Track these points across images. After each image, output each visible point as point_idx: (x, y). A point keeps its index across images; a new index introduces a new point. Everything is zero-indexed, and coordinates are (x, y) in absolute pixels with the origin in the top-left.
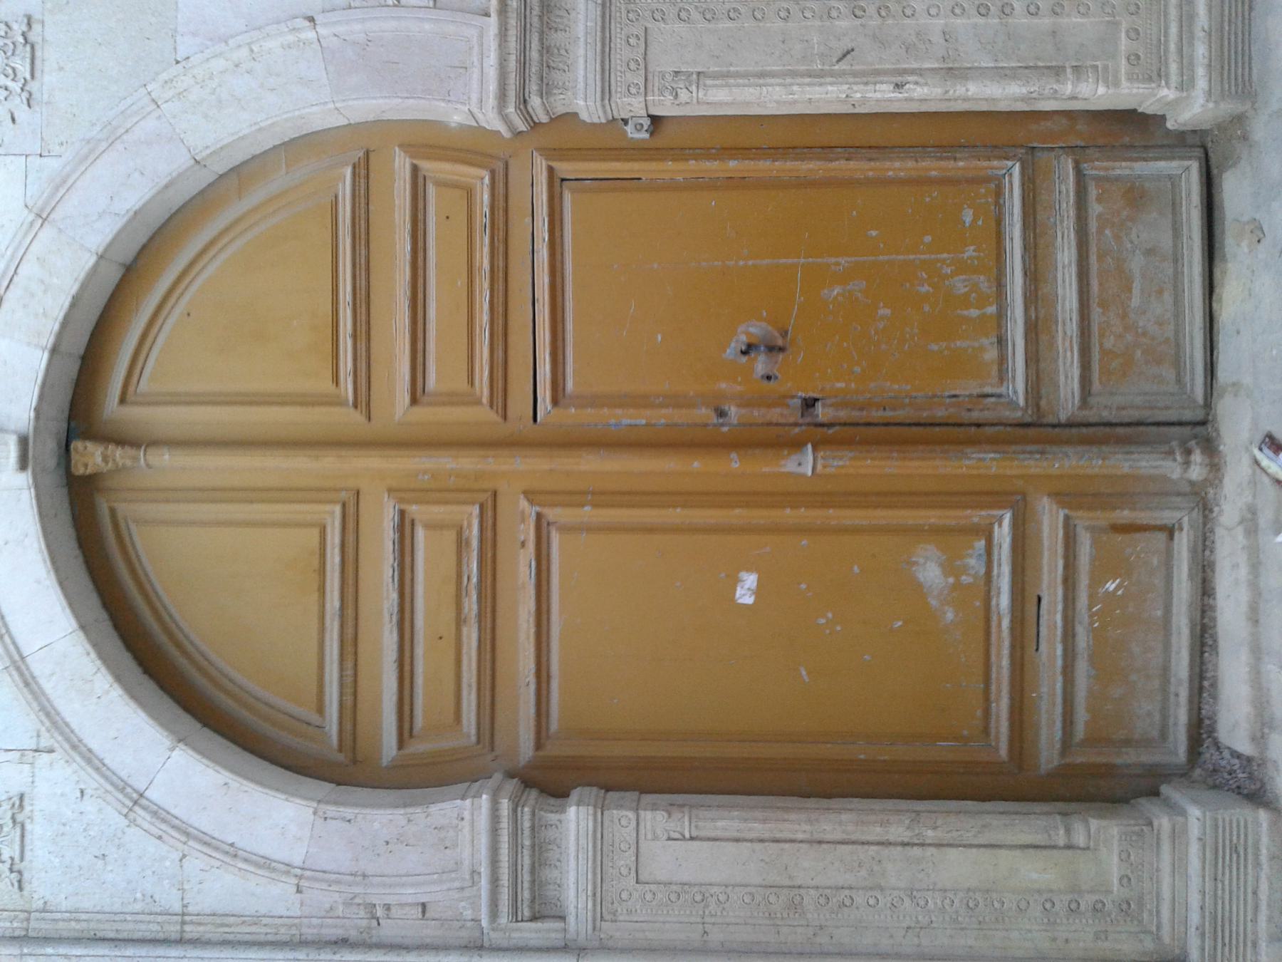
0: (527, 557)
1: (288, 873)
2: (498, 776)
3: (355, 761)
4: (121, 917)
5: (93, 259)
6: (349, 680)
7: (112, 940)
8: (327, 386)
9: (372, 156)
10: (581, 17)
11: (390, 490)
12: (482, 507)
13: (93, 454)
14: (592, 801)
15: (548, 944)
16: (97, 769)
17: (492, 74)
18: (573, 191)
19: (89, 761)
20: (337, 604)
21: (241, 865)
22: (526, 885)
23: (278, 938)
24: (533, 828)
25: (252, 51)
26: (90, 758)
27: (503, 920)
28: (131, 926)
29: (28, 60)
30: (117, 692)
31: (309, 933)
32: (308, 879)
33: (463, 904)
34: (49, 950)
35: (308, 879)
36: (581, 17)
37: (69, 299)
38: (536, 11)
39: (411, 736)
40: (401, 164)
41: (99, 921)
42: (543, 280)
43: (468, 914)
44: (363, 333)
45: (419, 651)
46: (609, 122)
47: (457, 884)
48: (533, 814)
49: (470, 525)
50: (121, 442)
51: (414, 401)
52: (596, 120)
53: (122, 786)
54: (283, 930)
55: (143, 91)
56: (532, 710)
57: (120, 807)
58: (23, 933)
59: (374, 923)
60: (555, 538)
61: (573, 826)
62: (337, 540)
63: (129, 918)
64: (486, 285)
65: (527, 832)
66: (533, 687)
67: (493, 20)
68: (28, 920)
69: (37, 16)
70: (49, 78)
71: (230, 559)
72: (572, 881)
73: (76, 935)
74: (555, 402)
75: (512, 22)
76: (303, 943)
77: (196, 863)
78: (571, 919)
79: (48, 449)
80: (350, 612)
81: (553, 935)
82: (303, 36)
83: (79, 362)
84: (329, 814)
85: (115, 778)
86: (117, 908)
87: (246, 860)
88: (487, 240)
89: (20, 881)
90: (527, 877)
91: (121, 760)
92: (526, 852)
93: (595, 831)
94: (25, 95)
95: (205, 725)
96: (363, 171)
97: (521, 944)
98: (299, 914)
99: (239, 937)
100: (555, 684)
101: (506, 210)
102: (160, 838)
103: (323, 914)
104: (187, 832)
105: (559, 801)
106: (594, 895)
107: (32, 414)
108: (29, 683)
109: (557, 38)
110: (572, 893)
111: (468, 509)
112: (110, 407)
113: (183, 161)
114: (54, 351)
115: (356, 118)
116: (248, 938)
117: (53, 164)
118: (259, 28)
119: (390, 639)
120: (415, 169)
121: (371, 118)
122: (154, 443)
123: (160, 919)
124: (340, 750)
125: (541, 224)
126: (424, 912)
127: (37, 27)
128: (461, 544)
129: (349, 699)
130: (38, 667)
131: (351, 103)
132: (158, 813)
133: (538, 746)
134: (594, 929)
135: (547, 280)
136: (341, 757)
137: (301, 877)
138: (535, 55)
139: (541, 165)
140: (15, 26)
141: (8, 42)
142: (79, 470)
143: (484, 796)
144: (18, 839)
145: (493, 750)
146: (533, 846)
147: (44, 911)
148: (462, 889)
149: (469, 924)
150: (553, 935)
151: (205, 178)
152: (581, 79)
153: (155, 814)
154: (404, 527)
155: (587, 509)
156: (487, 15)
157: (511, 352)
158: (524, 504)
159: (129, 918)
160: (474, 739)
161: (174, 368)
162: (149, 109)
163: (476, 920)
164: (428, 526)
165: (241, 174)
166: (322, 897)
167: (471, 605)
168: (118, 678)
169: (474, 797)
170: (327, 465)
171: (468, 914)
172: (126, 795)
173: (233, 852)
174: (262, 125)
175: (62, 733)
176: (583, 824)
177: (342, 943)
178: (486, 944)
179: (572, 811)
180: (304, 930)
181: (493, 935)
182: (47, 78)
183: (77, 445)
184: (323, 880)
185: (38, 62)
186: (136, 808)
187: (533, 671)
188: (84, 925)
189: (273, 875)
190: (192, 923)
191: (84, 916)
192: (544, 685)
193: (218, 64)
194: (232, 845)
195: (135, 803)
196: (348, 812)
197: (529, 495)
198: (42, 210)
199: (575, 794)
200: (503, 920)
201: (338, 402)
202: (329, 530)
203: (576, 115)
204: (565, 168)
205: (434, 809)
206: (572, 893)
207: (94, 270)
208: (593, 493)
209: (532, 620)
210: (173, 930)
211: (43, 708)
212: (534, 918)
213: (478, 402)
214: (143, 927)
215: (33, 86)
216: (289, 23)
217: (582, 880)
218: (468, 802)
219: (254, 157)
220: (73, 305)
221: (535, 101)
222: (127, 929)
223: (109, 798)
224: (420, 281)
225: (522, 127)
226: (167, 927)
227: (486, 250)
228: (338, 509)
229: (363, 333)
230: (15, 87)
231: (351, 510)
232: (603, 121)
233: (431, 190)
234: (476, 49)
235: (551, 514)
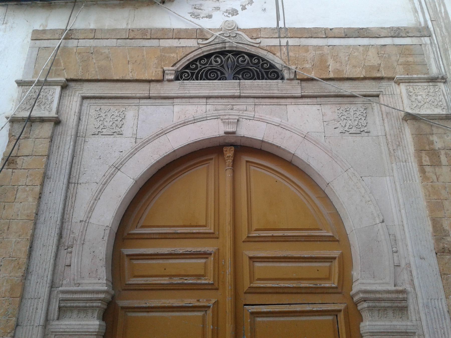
0: (192, 302)
1: (88, 217)
2: (113, 292)
3: (124, 239)
4: (79, 164)
5: (293, 153)
6: (152, 236)
7: (72, 162)
8: (255, 226)
9: (337, 243)
10: (400, 323)
11: (218, 249)
12: (212, 284)
13: (230, 153)
14: (100, 331)
15: (49, 314)
16: (129, 156)
17: (373, 288)
18: (333, 320)
19: (131, 154)
20: (179, 231)
21: (92, 202)
22: (72, 304)
23: (65, 215)
24: (93, 307)
25: (369, 201)
26: (132, 154)
27: (61, 296)
28: (76, 167)
29: (355, 132)
30: (153, 162)
31: (66, 225)
32: (85, 224)
33: (68, 280)
34: (72, 143)
35: (85, 224)
36: (400, 323)
37: (279, 146)
38: (399, 305)
39: (131, 259)
40: (336, 253)
41: (79, 157)
42: (298, 308)
43: (65, 282)
44: (274, 239)
45: (161, 261)
46: (361, 334)
47: (76, 278)
48: (98, 307)
49: (206, 279)
50: (234, 161)
51: (250, 258)
52: (361, 329)
53: (122, 164)
54: (68, 216)
55: (350, 167)
56: (136, 305)
57: (116, 163)
58: (78, 135)
59: (66, 248)
60: (200, 314)
61: (91, 323)
62: (201, 231)
63: (79, 166)
64: (294, 285)
65: (91, 304)
66: (144, 305)
67: (392, 288)
68: (82, 137)
69: (370, 134)
70: (350, 138)
71: (195, 199)
72: (71, 323)
73: (76, 151)
74: (252, 313)
75: (394, 296)
76: (62, 223)
77: (95, 187)
78: (57, 322)
79: (231, 140)
80: (177, 236)
81: (52, 315)
82: (377, 218)
83: (260, 148)
84: (106, 231)
85: (125, 161)
86: (83, 163)
87: (93, 203)
88: (311, 285)
89: (95, 134)
90: (75, 305)
91: (131, 163)
92: (84, 304)
93: (89, 332)
94: (344, 131)
95: (140, 189)
96: (331, 239)
97: (51, 303)
98: (73, 221)
99: (67, 202)
100: (145, 314)
101: (323, 293)
102: (104, 176)
103: (71, 230)
104: (105, 184)
105: (101, 317)
106: (65, 332)
107: (242, 135)
108: (158, 136)
109: (390, 313)
110: (67, 323)
111: (212, 279)
112: (246, 158)
113: (328, 180)
114: (262, 141)
115: (350, 237)
116: (67, 204)
117: (323, 139)
118: (377, 204)
119: (165, 250)
120: (335, 258)
121: (351, 242)
122: (234, 172)
123: (77, 176)
124: (129, 234)
125: (319, 307)
126: (67, 266)
127: (366, 134)
128: (199, 276)
129: (146, 236)
130: (163, 138)
131: (355, 235)
132: (113, 175)
133: (123, 308)
134: (52, 332)
135: (298, 309)
136: (125, 234)
137: (85, 222)
138: (383, 304)
139: (341, 307)
140: (366, 128)
141: (360, 126)
142: (224, 149)
143: (106, 288)
144: (109, 133)
145: (123, 290)
146: (86, 307)
147: (85, 141)
148: (74, 280)
149: (61, 282)
150: (52, 315)
151: (323, 187)
152: (376, 323)
153: (112, 174)
154: (205, 255)
155: (212, 326)
156: (395, 286)
157: (270, 295)
158: (213, 301)
159: (79, 166)
160: (127, 283)
161: (260, 179)
162: (344, 168)
163: (62, 285)
164: (205, 263)
165: (325, 198)
166: (77, 229)
167: (176, 280)
168: (158, 162)
169: (106, 284)
170: (227, 228)
171: (65, 282)
172: (119, 165)
173: (97, 199)
174: (344, 205)
175: (141, 145)
176: (92, 327)
177: (60, 236)
178: (53, 289)
179: (97, 322)
180: (67, 223)
181: (56, 292)
182: (350, 137)
183: (233, 148)
184: (83, 229)
185: (355, 135)
186: (115, 168)
187: (150, 305)
188: (78, 153)
189: (87, 213)
190: (75, 186)
191: (81, 153)
192: (145, 310)
193: (363, 191)
194: (99, 199)
195: (117, 168)
196: (106, 238)
197: (217, 303)
198: (307, 137)
199: (103, 323)
200: (61, 296)
201: (249, 231)
202: (204, 228)
203: (362, 321)
204: (341, 316)
205: (104, 269)
206: (67, 323)
207: (290, 153)
208: (217, 329)
209: (170, 305)
210: (73, 180)
211: (149, 140)
212: (60, 308)
213: (251, 283)
214: (75, 171)
215: (347, 134)
216: (380, 214)
217: (71, 327)
218: (105, 282)
219: (332, 202)
220: (277, 146)
221: (365, 305)
222: (75, 167)
223: (119, 160)
224: (294, 260)
225: (355, 299)
226: (74, 178)
227: (308, 285)
228: (212, 231)
229: (274, 239)
230: (346, 129)
231: (211, 236)
232: (361, 332)
233: (327, 264)
234: (381, 281)
235: (210, 312)
